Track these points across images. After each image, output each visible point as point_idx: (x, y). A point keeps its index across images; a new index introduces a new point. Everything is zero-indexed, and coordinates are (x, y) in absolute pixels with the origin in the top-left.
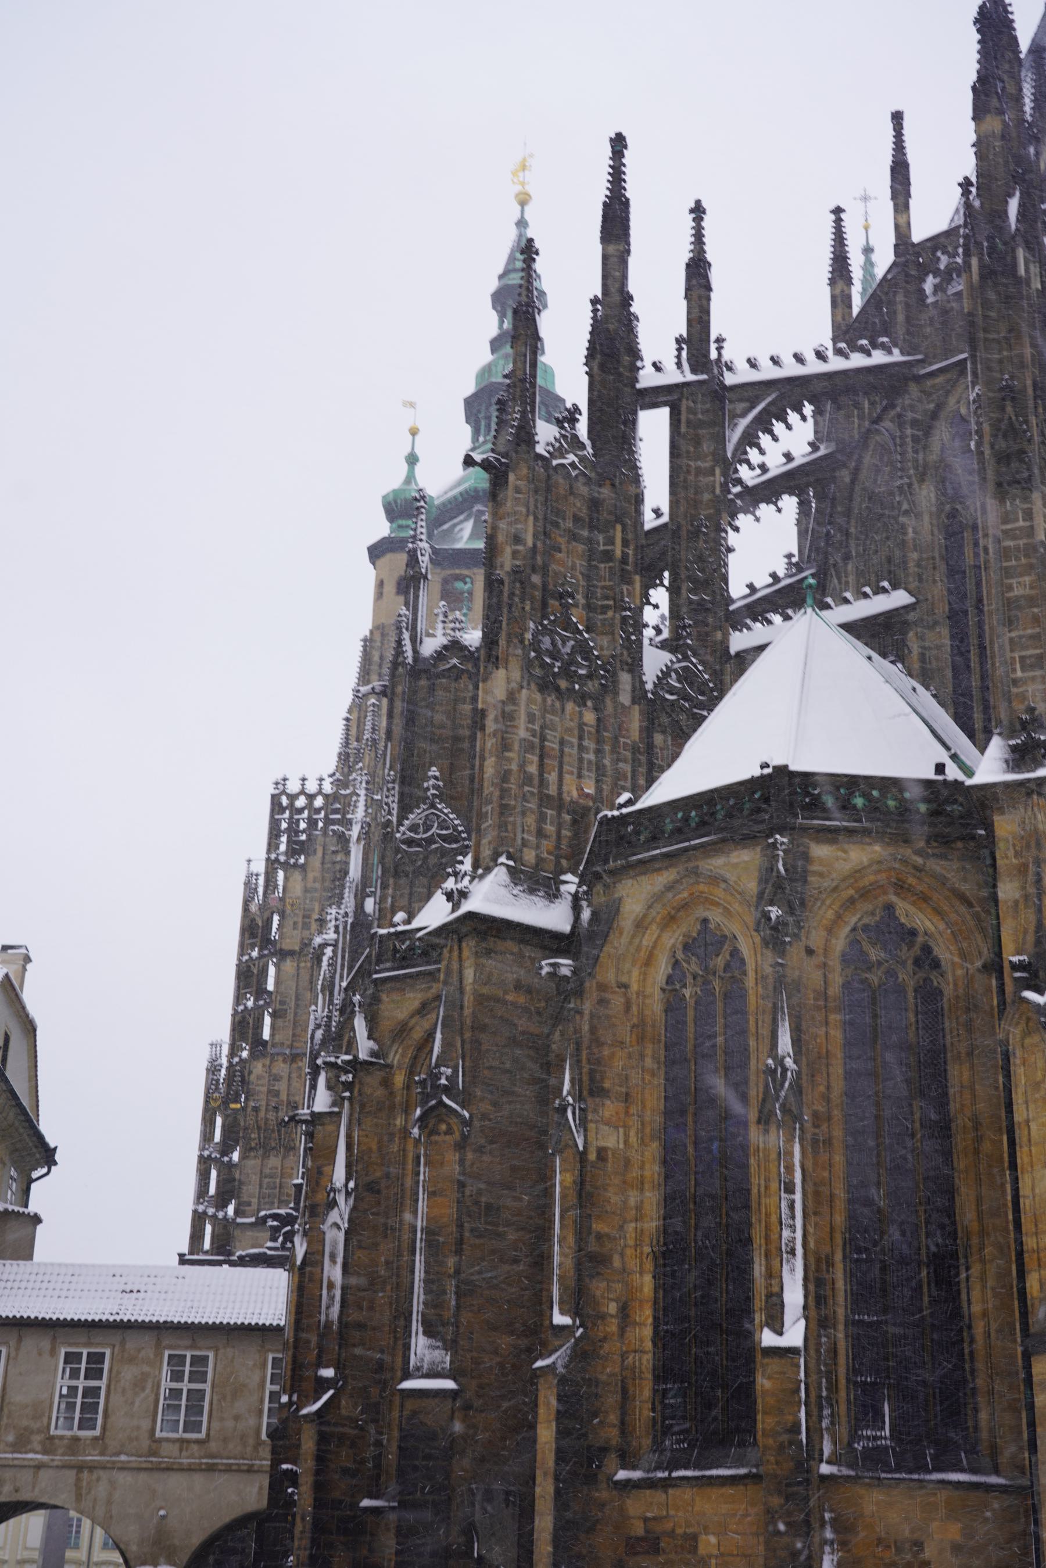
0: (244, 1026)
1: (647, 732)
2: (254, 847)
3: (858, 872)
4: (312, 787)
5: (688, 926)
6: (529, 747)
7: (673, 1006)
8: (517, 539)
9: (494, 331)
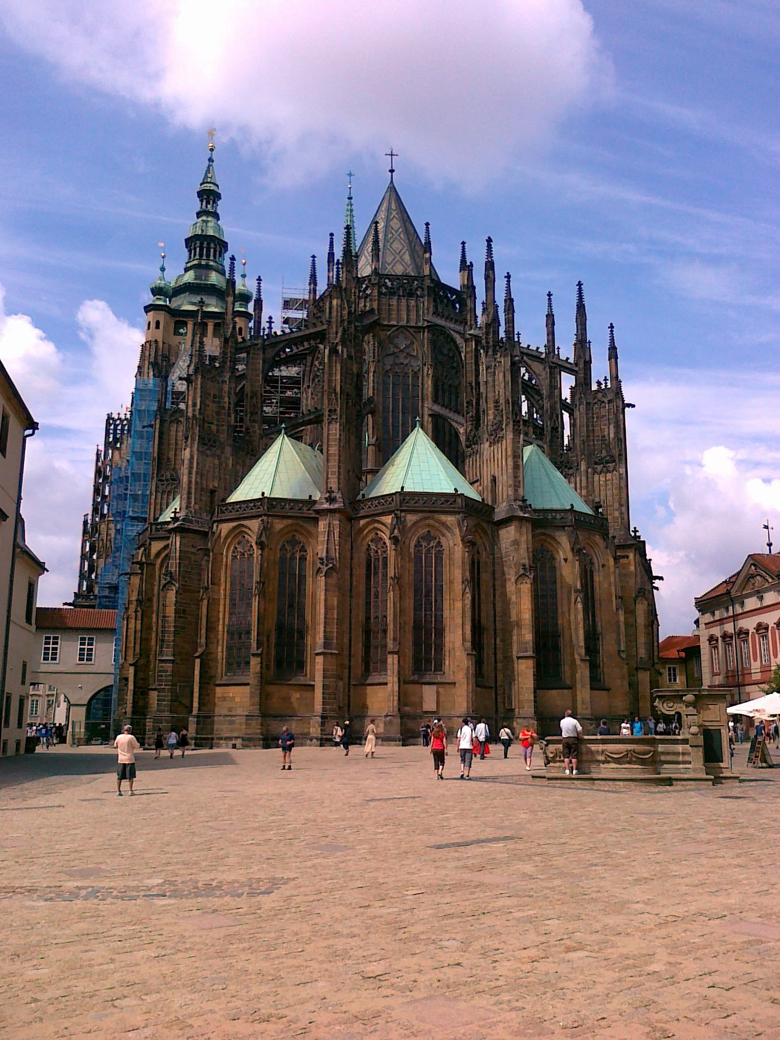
0: (96, 509)
2: (100, 441)
3: (286, 527)
9: (198, 209)
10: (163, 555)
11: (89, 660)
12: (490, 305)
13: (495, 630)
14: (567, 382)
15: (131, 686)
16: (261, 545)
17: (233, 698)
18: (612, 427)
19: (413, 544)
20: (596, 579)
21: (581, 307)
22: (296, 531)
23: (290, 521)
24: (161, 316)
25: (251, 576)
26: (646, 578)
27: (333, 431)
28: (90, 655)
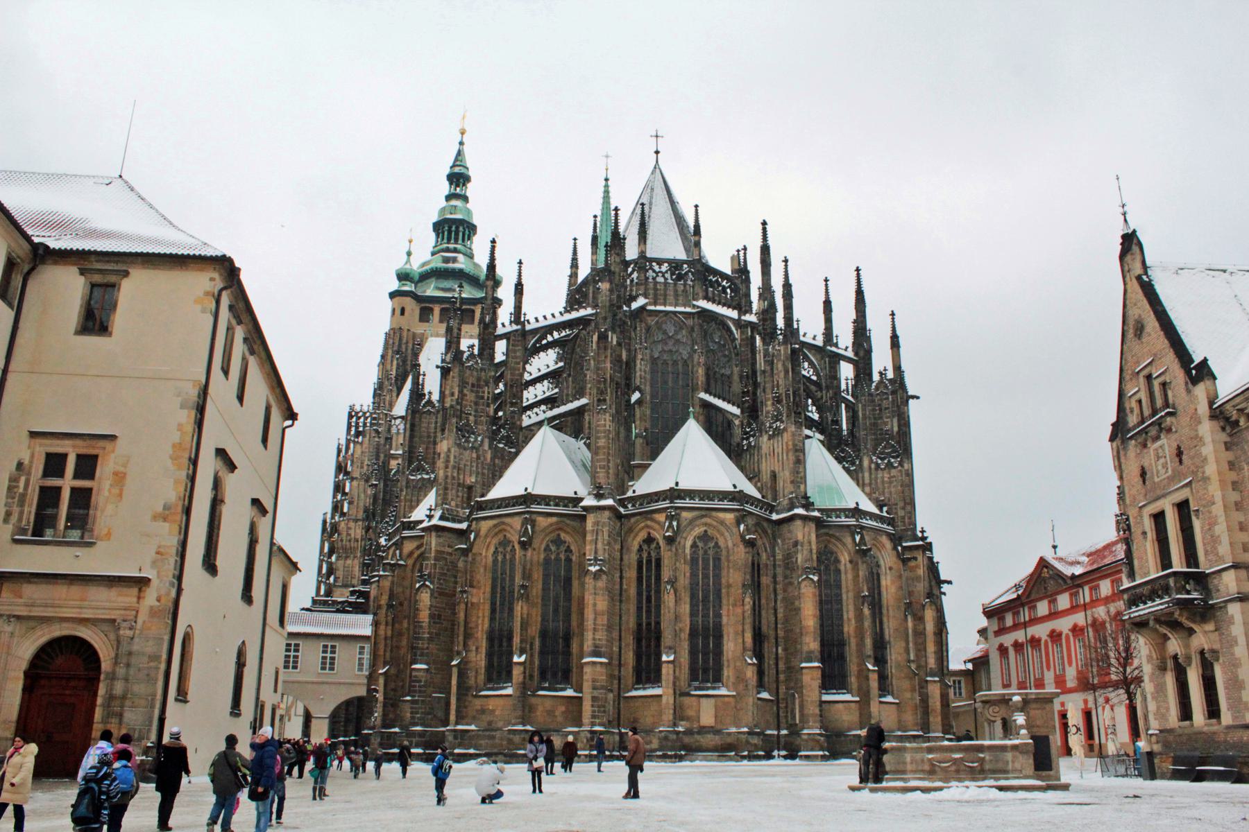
0: (337, 507)
1: (493, 459)
3: (551, 525)
4: (365, 409)
5: (501, 536)
6: (454, 467)
7: (495, 561)
8: (452, 394)
9: (447, 193)
10: (415, 555)
11: (332, 669)
12: (766, 291)
13: (776, 639)
14: (846, 371)
15: (380, 696)
16: (524, 545)
17: (493, 711)
18: (895, 420)
19: (689, 543)
20: (883, 583)
21: (860, 293)
22: (560, 529)
23: (554, 519)
24: (409, 303)
25: (512, 579)
26: (933, 583)
27: (604, 422)
28: (332, 664)
